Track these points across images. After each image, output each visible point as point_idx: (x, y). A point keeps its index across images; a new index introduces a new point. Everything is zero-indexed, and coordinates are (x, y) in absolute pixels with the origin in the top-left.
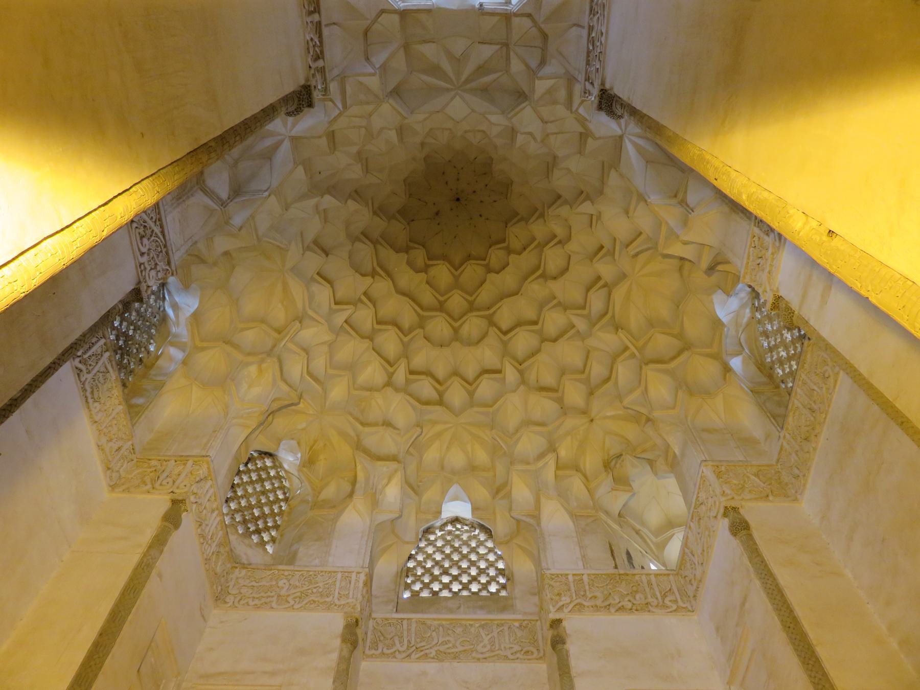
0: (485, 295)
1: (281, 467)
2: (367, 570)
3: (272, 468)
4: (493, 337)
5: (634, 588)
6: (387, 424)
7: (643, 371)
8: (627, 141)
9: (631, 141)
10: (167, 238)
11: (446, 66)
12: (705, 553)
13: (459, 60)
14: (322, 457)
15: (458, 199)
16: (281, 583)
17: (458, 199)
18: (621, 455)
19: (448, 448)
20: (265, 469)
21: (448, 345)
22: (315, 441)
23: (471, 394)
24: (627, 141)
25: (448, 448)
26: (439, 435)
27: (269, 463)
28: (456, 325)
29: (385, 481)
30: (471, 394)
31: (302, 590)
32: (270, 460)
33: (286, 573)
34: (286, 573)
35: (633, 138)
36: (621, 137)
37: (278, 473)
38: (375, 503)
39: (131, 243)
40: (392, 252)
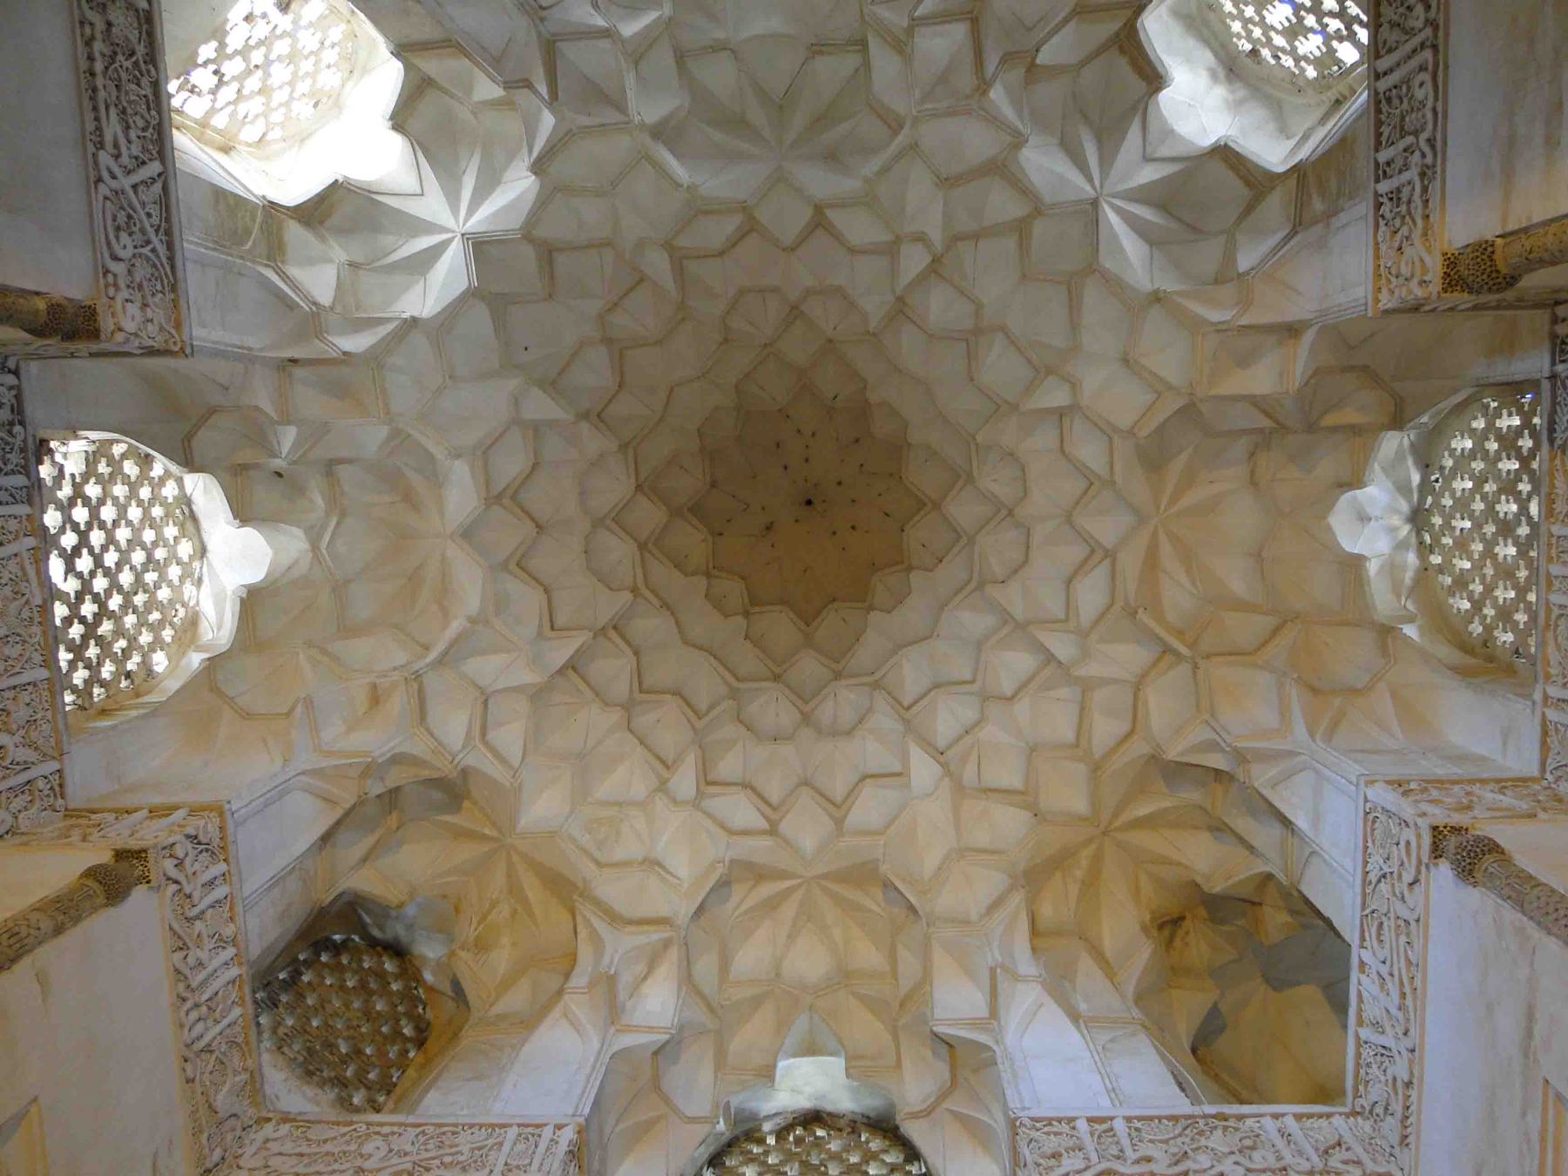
0: (864, 655)
1: (418, 979)
2: (581, 1120)
3: (397, 977)
4: (884, 719)
5: (1248, 1142)
6: (652, 864)
7: (1200, 673)
8: (1106, 206)
9: (1119, 211)
10: (180, 274)
11: (756, 115)
12: (1409, 1001)
13: (781, 107)
14: (505, 940)
15: (809, 502)
16: (368, 1148)
17: (809, 502)
18: (1182, 918)
19: (791, 937)
20: (381, 975)
21: (790, 738)
22: (494, 904)
23: (839, 823)
24: (1106, 206)
25: (791, 937)
26: (771, 905)
27: (389, 966)
28: (807, 709)
29: (640, 968)
30: (839, 823)
31: (416, 1158)
32: (396, 962)
33: (386, 1130)
34: (386, 1130)
35: (1119, 203)
36: (1095, 203)
37: (408, 988)
38: (613, 1013)
39: (91, 216)
40: (677, 574)
